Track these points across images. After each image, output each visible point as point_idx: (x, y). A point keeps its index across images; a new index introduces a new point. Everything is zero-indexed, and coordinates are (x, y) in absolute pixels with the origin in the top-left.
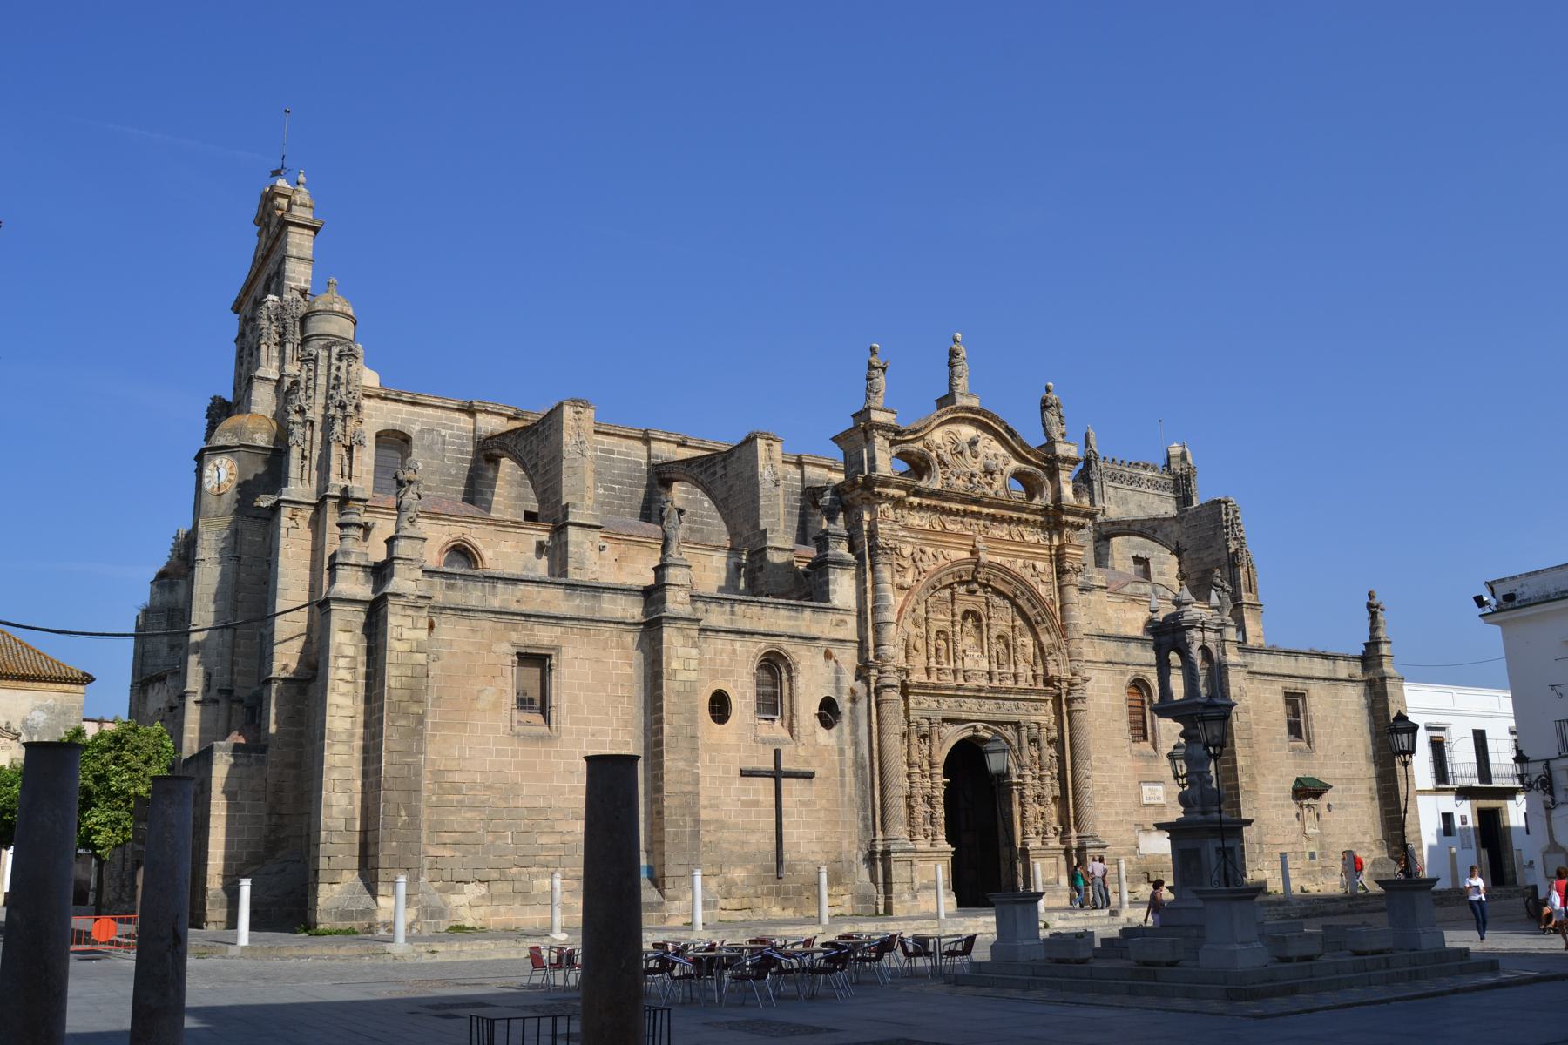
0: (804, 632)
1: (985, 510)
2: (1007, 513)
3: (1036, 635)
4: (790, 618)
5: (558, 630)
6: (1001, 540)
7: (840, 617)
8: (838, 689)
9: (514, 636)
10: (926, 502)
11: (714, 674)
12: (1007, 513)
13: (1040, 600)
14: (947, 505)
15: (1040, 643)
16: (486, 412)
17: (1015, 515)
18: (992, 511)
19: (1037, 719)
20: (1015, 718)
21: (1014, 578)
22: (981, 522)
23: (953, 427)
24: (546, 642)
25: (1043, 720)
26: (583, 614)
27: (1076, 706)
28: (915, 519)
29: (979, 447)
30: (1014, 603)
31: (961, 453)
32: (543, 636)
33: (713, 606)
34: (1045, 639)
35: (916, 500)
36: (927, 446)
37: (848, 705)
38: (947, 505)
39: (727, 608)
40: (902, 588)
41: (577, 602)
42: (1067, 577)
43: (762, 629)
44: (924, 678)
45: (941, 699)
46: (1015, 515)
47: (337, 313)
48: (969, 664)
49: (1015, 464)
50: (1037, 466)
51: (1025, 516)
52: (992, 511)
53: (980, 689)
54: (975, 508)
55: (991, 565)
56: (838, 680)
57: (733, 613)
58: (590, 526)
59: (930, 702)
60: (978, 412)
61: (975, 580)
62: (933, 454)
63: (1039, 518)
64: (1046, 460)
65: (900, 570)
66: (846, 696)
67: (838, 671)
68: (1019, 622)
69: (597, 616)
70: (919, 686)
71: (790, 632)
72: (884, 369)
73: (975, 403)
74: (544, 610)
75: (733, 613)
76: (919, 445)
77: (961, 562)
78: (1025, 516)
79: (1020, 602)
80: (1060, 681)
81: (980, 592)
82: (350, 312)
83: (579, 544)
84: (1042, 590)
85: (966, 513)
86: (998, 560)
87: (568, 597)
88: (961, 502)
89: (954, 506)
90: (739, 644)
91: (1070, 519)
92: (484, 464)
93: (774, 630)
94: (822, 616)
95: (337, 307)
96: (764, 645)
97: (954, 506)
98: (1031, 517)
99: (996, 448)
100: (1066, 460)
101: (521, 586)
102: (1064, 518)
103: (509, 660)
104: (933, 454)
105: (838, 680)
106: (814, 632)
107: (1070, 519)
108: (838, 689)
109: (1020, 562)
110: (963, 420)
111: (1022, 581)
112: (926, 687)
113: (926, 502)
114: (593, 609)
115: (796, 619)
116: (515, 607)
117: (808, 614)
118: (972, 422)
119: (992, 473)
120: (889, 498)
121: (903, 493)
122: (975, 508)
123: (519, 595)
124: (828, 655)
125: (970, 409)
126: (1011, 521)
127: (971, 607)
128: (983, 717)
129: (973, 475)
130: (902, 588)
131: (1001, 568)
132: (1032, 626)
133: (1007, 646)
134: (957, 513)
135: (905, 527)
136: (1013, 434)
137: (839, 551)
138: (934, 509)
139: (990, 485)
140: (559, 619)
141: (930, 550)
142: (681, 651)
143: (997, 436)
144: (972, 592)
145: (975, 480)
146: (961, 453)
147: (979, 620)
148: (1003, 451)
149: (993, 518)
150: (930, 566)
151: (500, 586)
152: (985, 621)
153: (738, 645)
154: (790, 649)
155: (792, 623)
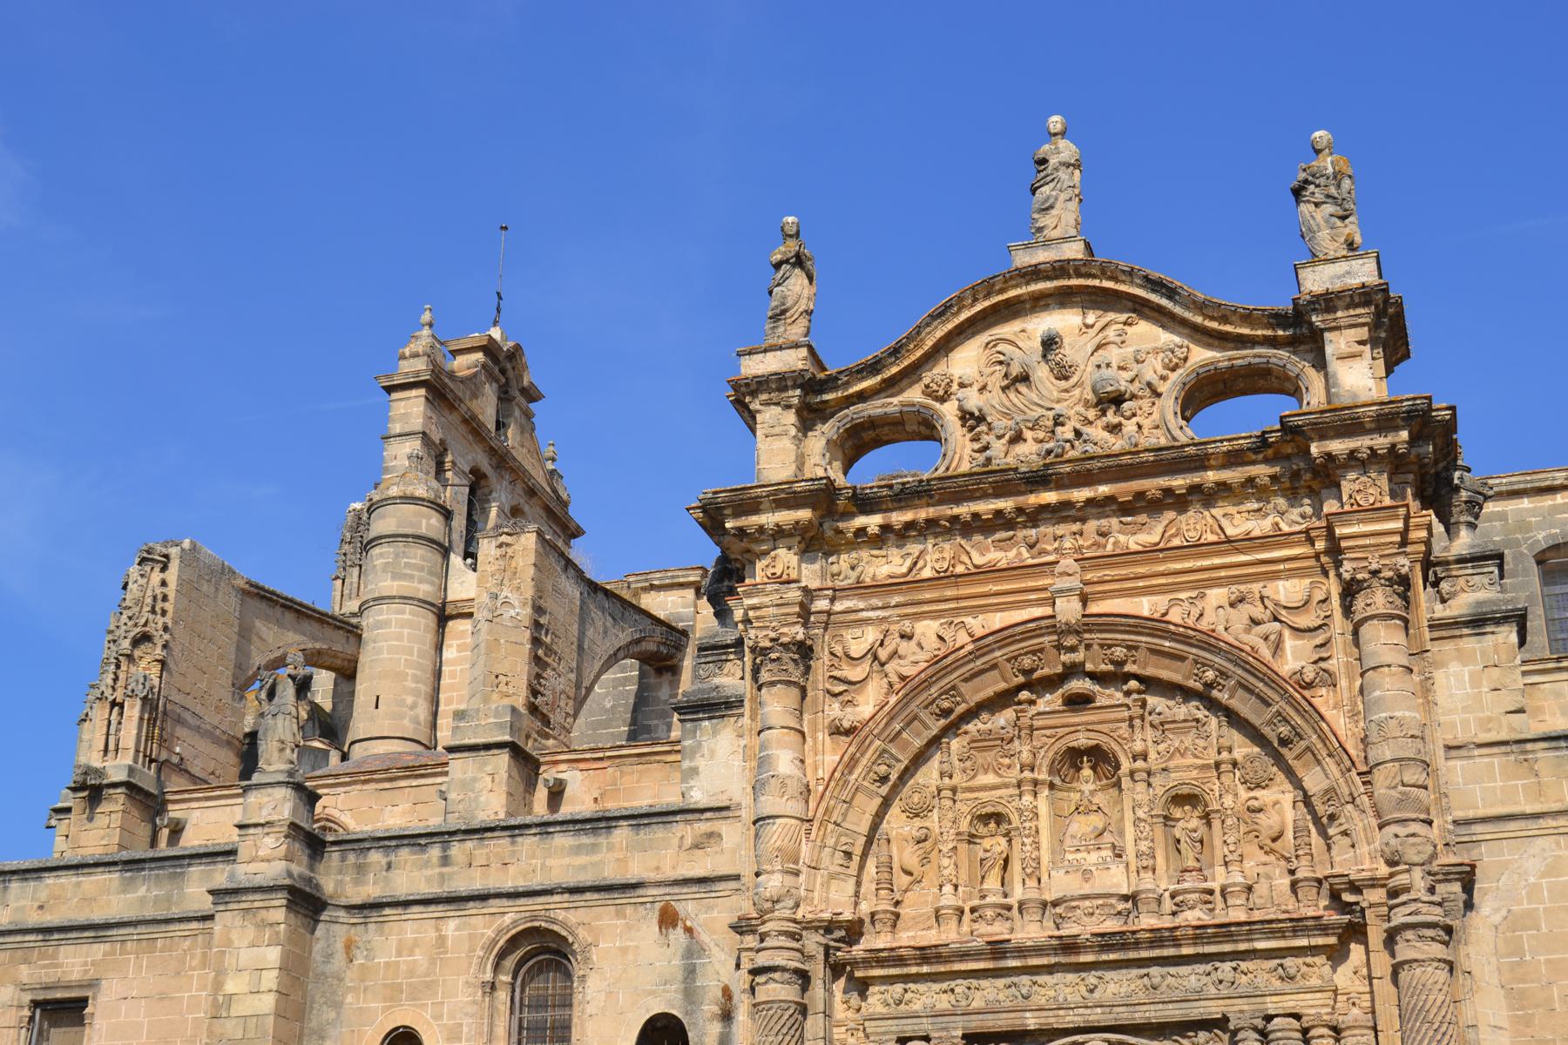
0: (611, 874)
1: (1080, 495)
2: (1153, 485)
3: (1297, 784)
4: (577, 850)
5: (99, 950)
6: (1150, 553)
7: (703, 827)
8: (690, 993)
9: (25, 973)
10: (899, 518)
11: (393, 994)
12: (1153, 485)
13: (1272, 679)
14: (964, 510)
15: (1307, 800)
16: (652, 587)
17: (1179, 482)
18: (1104, 490)
19: (1289, 1003)
20: (1213, 1010)
21: (1184, 639)
22: (1092, 525)
23: (1007, 330)
24: (75, 975)
25: (1313, 1005)
26: (149, 913)
27: (1404, 952)
28: (888, 564)
29: (1075, 350)
30: (1213, 706)
31: (1024, 378)
32: (72, 964)
33: (404, 853)
34: (1314, 781)
35: (873, 522)
36: (928, 392)
37: (716, 1028)
38: (964, 510)
39: (435, 852)
40: (837, 731)
41: (142, 891)
42: (1359, 603)
43: (508, 885)
44: (930, 937)
45: (960, 985)
46: (1179, 482)
47: (391, 501)
48: (1060, 884)
49: (1201, 355)
50: (1272, 342)
51: (1211, 476)
52: (1104, 490)
53: (1069, 946)
54: (1050, 497)
55: (1092, 624)
56: (690, 972)
57: (445, 861)
58: (487, 747)
59: (927, 997)
60: (1060, 269)
61: (1073, 670)
62: (949, 411)
63: (1262, 471)
64: (1278, 319)
65: (846, 690)
66: (710, 1008)
67: (694, 952)
68: (1243, 749)
69: (176, 911)
70: (876, 958)
71: (572, 880)
72: (799, 261)
73: (1074, 251)
74: (81, 918)
75: (445, 861)
76: (914, 395)
77: (1005, 636)
78: (1211, 476)
79: (1222, 696)
80: (1355, 888)
81: (1109, 696)
82: (421, 491)
83: (466, 785)
84: (1294, 657)
85: (1036, 516)
86: (1145, 606)
87: (126, 886)
88: (1001, 491)
89: (985, 507)
90: (452, 926)
91: (1338, 446)
92: (652, 680)
93: (535, 883)
94: (658, 833)
95: (394, 491)
96: (511, 917)
97: (985, 507)
98: (1233, 475)
99: (1146, 333)
100: (1328, 302)
101: (50, 880)
102: (1314, 449)
103: (12, 1017)
104: (949, 411)
105: (690, 972)
106: (635, 870)
107: (1338, 446)
108: (690, 993)
109: (1217, 595)
110: (1038, 303)
111: (1209, 642)
112: (901, 961)
113: (899, 518)
114: (169, 899)
115: (594, 848)
116: (35, 919)
117: (622, 833)
118: (1064, 298)
119: (1117, 400)
120: (779, 534)
121: (804, 514)
122: (1050, 497)
123: (43, 895)
124: (668, 919)
125: (1034, 273)
126: (1178, 502)
127: (1082, 740)
128: (1097, 1016)
129: (1058, 421)
130: (837, 731)
131: (1156, 626)
132: (1275, 750)
133: (1207, 818)
134: (1001, 521)
135: (860, 589)
136: (1171, 293)
137: (717, 681)
138: (930, 527)
139: (1114, 429)
140: (97, 930)
141: (927, 629)
142: (246, 956)
143: (1141, 308)
144: (1078, 702)
145: (1066, 432)
146: (1024, 378)
147: (1118, 766)
148: (1166, 338)
149: (1126, 509)
150: (912, 661)
151: (15, 886)
152: (1126, 765)
153: (450, 927)
154: (572, 917)
155: (583, 859)
